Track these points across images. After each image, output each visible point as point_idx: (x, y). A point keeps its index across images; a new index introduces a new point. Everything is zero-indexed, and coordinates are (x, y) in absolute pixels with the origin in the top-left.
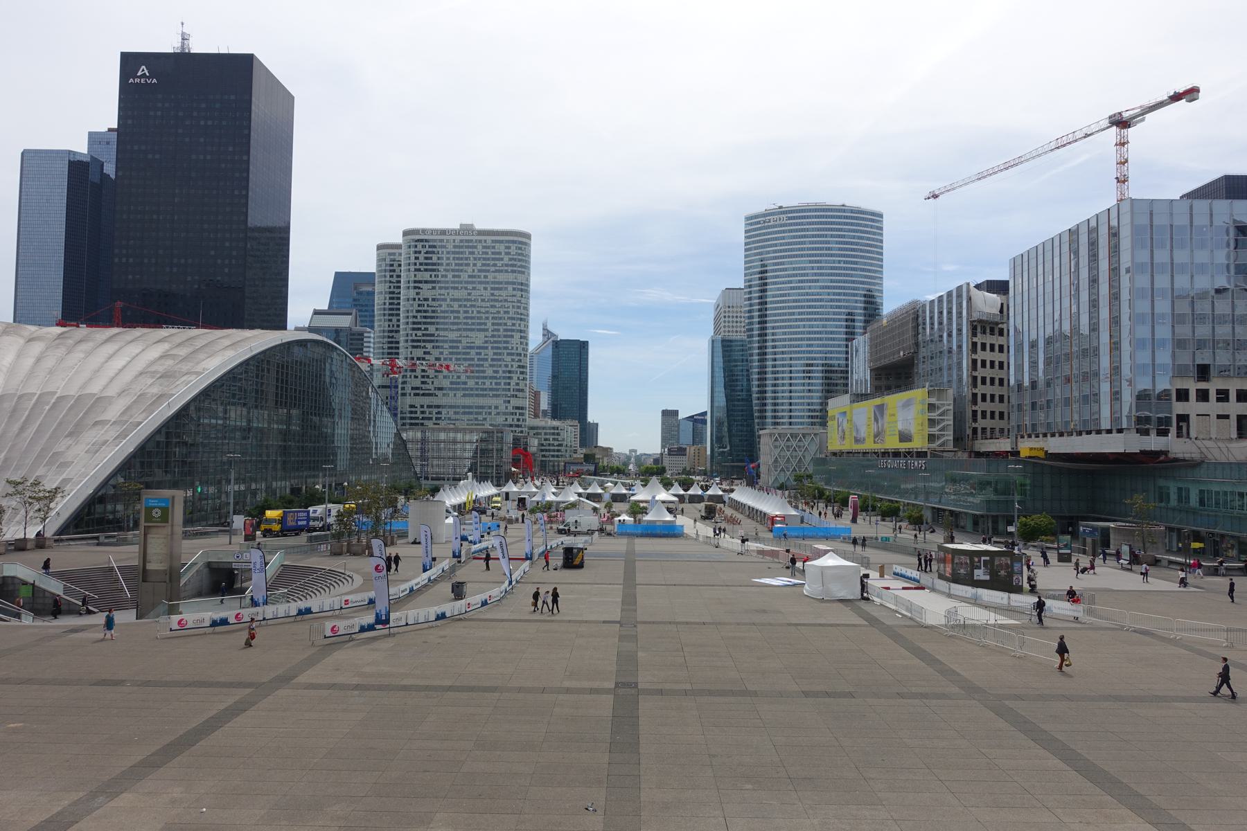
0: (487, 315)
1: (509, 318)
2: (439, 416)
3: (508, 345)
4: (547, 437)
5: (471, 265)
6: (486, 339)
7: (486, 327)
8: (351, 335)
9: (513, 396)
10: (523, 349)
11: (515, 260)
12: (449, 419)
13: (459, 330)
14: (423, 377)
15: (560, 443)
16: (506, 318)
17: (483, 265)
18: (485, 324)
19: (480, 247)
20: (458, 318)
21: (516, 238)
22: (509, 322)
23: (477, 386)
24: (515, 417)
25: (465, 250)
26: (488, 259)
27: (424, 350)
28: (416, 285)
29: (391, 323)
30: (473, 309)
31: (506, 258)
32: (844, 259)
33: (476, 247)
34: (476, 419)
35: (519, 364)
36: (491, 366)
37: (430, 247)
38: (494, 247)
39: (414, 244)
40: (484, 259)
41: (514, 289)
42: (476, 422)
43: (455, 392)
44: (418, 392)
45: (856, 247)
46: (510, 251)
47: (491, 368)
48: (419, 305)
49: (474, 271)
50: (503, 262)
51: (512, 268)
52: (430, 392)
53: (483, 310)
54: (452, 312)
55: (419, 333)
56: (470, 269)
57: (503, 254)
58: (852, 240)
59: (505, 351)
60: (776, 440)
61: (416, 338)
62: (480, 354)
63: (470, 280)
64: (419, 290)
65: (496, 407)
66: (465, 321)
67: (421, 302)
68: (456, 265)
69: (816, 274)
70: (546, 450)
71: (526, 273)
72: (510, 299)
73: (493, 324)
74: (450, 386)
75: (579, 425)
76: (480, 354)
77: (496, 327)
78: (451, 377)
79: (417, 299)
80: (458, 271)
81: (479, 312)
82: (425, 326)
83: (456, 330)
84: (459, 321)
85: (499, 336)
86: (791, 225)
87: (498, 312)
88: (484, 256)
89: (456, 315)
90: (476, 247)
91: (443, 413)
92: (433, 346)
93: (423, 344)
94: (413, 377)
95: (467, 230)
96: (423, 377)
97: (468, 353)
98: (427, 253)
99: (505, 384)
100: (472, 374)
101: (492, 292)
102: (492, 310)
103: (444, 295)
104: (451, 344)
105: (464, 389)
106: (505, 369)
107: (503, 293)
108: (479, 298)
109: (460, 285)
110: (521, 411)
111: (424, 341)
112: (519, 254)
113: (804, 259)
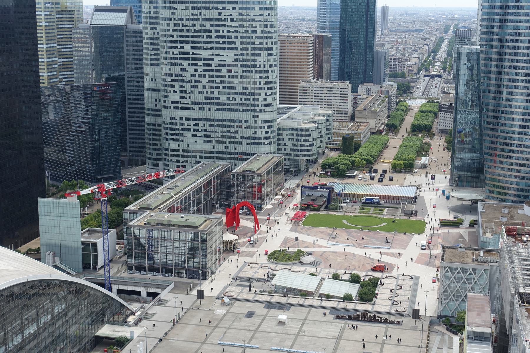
0: (236, 34)
1: (257, 37)
2: (196, 128)
3: (256, 63)
6: (236, 57)
7: (235, 46)
8: (127, 32)
10: (271, 66)
12: (205, 131)
13: (212, 48)
14: (181, 92)
15: (311, 143)
16: (254, 37)
18: (235, 43)
20: (211, 37)
22: (257, 42)
23: (229, 102)
27: (181, 67)
28: (172, 5)
29: (155, 31)
35: (266, 80)
36: (241, 83)
41: (261, 9)
42: (229, 134)
43: (209, 106)
44: (177, 105)
48: (175, 25)
53: (232, 29)
54: (205, 31)
55: (176, 51)
60: (447, 272)
61: (173, 56)
64: (175, 11)
65: (246, 121)
66: (217, 40)
67: (176, 22)
70: (298, 150)
72: (257, 18)
73: (242, 43)
74: (205, 101)
75: (350, 85)
77: (245, 46)
79: (173, 19)
81: (229, 31)
82: (181, 45)
83: (209, 49)
84: (211, 40)
85: (248, 55)
87: (247, 32)
89: (208, 34)
92: (189, 64)
93: (179, 62)
94: (172, 92)
96: (181, 92)
99: (254, 100)
101: (241, 11)
102: (241, 29)
103: (197, 15)
104: (205, 62)
106: (253, 86)
107: (251, 13)
108: (229, 18)
109: (212, 5)
110: (269, 124)
111: (181, 59)
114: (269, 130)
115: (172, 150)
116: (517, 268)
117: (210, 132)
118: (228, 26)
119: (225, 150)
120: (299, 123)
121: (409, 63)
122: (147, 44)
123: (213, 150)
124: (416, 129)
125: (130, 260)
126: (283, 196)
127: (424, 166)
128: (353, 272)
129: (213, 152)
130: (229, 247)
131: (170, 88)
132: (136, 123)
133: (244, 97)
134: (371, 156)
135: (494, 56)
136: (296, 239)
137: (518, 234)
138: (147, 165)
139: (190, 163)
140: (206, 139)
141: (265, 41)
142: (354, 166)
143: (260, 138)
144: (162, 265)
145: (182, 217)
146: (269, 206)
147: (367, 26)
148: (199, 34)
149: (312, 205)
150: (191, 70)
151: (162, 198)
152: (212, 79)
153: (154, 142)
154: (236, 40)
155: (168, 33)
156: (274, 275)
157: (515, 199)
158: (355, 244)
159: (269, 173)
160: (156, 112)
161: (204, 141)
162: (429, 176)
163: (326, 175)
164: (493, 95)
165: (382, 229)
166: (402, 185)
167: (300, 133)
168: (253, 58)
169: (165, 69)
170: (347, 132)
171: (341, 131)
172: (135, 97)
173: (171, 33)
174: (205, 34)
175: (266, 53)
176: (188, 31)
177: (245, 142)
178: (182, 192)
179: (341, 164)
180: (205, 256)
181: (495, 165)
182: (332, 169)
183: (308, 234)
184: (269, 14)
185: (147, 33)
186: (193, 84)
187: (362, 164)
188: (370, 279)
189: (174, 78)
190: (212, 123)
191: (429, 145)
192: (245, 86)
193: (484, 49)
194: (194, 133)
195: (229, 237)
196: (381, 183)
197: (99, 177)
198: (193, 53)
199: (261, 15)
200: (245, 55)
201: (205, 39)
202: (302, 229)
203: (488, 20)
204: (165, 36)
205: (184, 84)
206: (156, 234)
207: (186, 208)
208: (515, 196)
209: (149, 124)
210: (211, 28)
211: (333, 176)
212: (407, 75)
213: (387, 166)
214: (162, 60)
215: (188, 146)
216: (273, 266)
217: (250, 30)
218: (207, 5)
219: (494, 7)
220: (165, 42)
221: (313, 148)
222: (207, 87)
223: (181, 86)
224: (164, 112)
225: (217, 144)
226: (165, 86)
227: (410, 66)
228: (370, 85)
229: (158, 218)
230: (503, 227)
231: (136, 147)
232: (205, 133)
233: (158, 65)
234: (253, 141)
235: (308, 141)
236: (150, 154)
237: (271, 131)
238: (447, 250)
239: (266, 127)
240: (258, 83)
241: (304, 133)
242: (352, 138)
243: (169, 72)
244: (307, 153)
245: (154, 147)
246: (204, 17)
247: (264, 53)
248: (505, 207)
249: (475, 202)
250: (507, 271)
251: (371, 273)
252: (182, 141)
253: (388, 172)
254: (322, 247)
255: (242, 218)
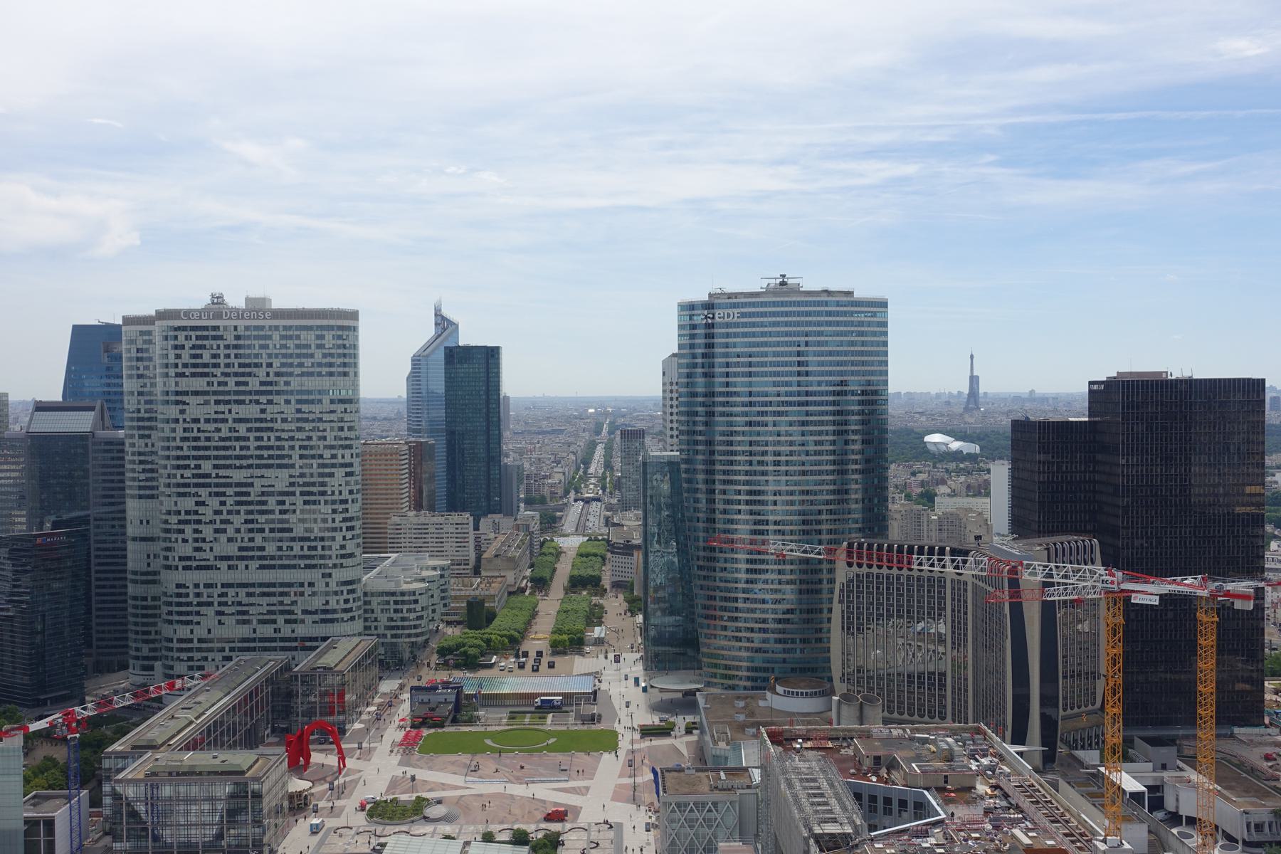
0: (291, 443)
1: (326, 447)
2: (223, 599)
3: (326, 489)
4: (399, 607)
5: (264, 365)
7: (291, 462)
8: (94, 444)
9: (335, 566)
10: (351, 492)
11: (331, 355)
12: (240, 604)
13: (250, 466)
14: (196, 540)
15: (419, 614)
16: (322, 447)
17: (283, 365)
18: (290, 457)
19: (276, 336)
20: (248, 448)
21: (332, 322)
22: (327, 454)
23: (280, 553)
24: (342, 598)
25: (254, 342)
26: (291, 356)
27: (196, 499)
28: (179, 398)
29: (147, 441)
30: (270, 434)
31: (318, 357)
32: (827, 378)
33: (270, 337)
34: (281, 603)
37: (198, 338)
38: (298, 337)
39: (172, 333)
40: (285, 356)
41: (332, 402)
42: (281, 608)
43: (246, 562)
44: (188, 563)
45: (845, 358)
46: (323, 342)
47: (301, 525)
48: (185, 430)
49: (268, 374)
50: (313, 360)
51: (328, 369)
52: (208, 563)
53: (285, 435)
54: (237, 439)
55: (187, 473)
56: (262, 372)
57: (313, 347)
58: (838, 349)
59: (322, 498)
60: (674, 811)
61: (182, 481)
62: (283, 503)
63: (264, 388)
64: (185, 407)
65: (311, 584)
66: (258, 452)
67: (186, 425)
68: (240, 365)
69: (784, 403)
70: (397, 628)
71: (352, 374)
72: (326, 417)
75: (471, 519)
76: (283, 503)
78: (239, 540)
79: (181, 421)
80: (243, 375)
81: (278, 439)
83: (245, 467)
84: (249, 453)
85: (312, 475)
86: (745, 325)
87: (310, 438)
88: (284, 351)
89: (243, 444)
90: (270, 337)
91: (229, 595)
92: (210, 493)
93: (193, 490)
94: (180, 540)
95: (257, 308)
96: (196, 540)
97: (264, 503)
98: (194, 347)
99: (323, 548)
100: (272, 535)
102: (298, 435)
103: (223, 413)
104: (237, 489)
105: (260, 558)
106: (322, 525)
107: (316, 408)
109: (250, 397)
110: (350, 587)
111: (196, 485)
112: (339, 347)
113: (766, 379)
114: (351, 597)
115: (180, 641)
116: (802, 795)
117: (247, 605)
118: (277, 431)
119: (275, 635)
120: (398, 583)
121: (550, 481)
122: (133, 462)
123: (254, 636)
124: (577, 583)
125: (118, 845)
126: (379, 705)
127: (599, 642)
128: (516, 827)
129: (254, 640)
130: (296, 802)
131: (175, 536)
132: (109, 598)
133: (306, 544)
134: (515, 630)
135: (701, 467)
136: (413, 778)
137: (786, 740)
138: (131, 670)
139: (213, 660)
140: (240, 617)
141: (340, 452)
142: (491, 647)
143: (334, 611)
144: (179, 847)
145: (215, 757)
146: (357, 726)
147: (488, 428)
148: (228, 444)
149: (431, 718)
150: (214, 503)
151: (173, 726)
152: (250, 517)
153: (145, 629)
154: (291, 452)
155: (173, 444)
156: (383, 845)
157: (749, 684)
158: (511, 778)
159: (357, 666)
160: (150, 577)
161: (238, 622)
162: (611, 656)
163: (446, 665)
164: (705, 525)
165: (550, 748)
166: (569, 674)
167: (399, 598)
168: (321, 480)
169: (168, 504)
170: (473, 593)
171: (463, 593)
172: (108, 553)
173: (178, 443)
174: (237, 444)
175: (342, 471)
176: (208, 439)
177: (309, 619)
178: (208, 713)
179: (470, 647)
180: (258, 823)
181: (715, 632)
182: (456, 655)
183: (430, 768)
184: (346, 409)
185: (133, 445)
186: (218, 526)
187: (502, 643)
188: (546, 836)
189: (183, 517)
190: (252, 590)
191: (601, 607)
192: (307, 525)
193: (683, 457)
194: (219, 609)
195: (298, 785)
196: (536, 674)
197: (42, 697)
198: (217, 474)
199: (332, 412)
200: (308, 475)
201: (238, 452)
202: (418, 760)
203: (688, 414)
204: (168, 448)
205: (200, 527)
206: (167, 791)
207: (216, 740)
208: (748, 678)
209: (135, 598)
210: (248, 434)
211: (457, 667)
212: (548, 499)
213: (543, 645)
214: (162, 489)
215: (209, 631)
216: (379, 829)
217: (315, 435)
218: (242, 398)
219: (694, 395)
220: (168, 458)
221: (423, 622)
222: (242, 530)
223: (196, 531)
224: (165, 576)
225: (261, 626)
226: (168, 531)
227: (552, 485)
228: (497, 517)
229: (170, 763)
230: (763, 730)
231: (110, 640)
232: (239, 608)
233: (152, 497)
234: (323, 616)
235: (415, 611)
236: (137, 649)
237: (354, 599)
238: (667, 774)
239: (345, 592)
240: (330, 521)
241: (406, 598)
242: (483, 602)
243: (175, 508)
244: (413, 631)
245: (145, 637)
246: (237, 416)
247: (340, 472)
248: (738, 698)
249: (690, 693)
250: (786, 800)
251: (544, 825)
252: (198, 623)
253: (544, 654)
254: (456, 788)
255: (314, 750)
